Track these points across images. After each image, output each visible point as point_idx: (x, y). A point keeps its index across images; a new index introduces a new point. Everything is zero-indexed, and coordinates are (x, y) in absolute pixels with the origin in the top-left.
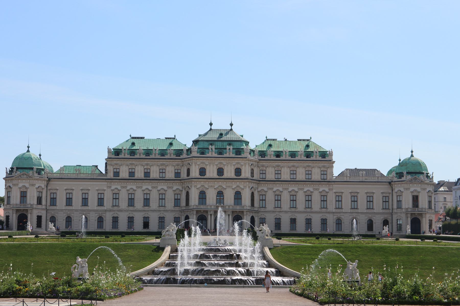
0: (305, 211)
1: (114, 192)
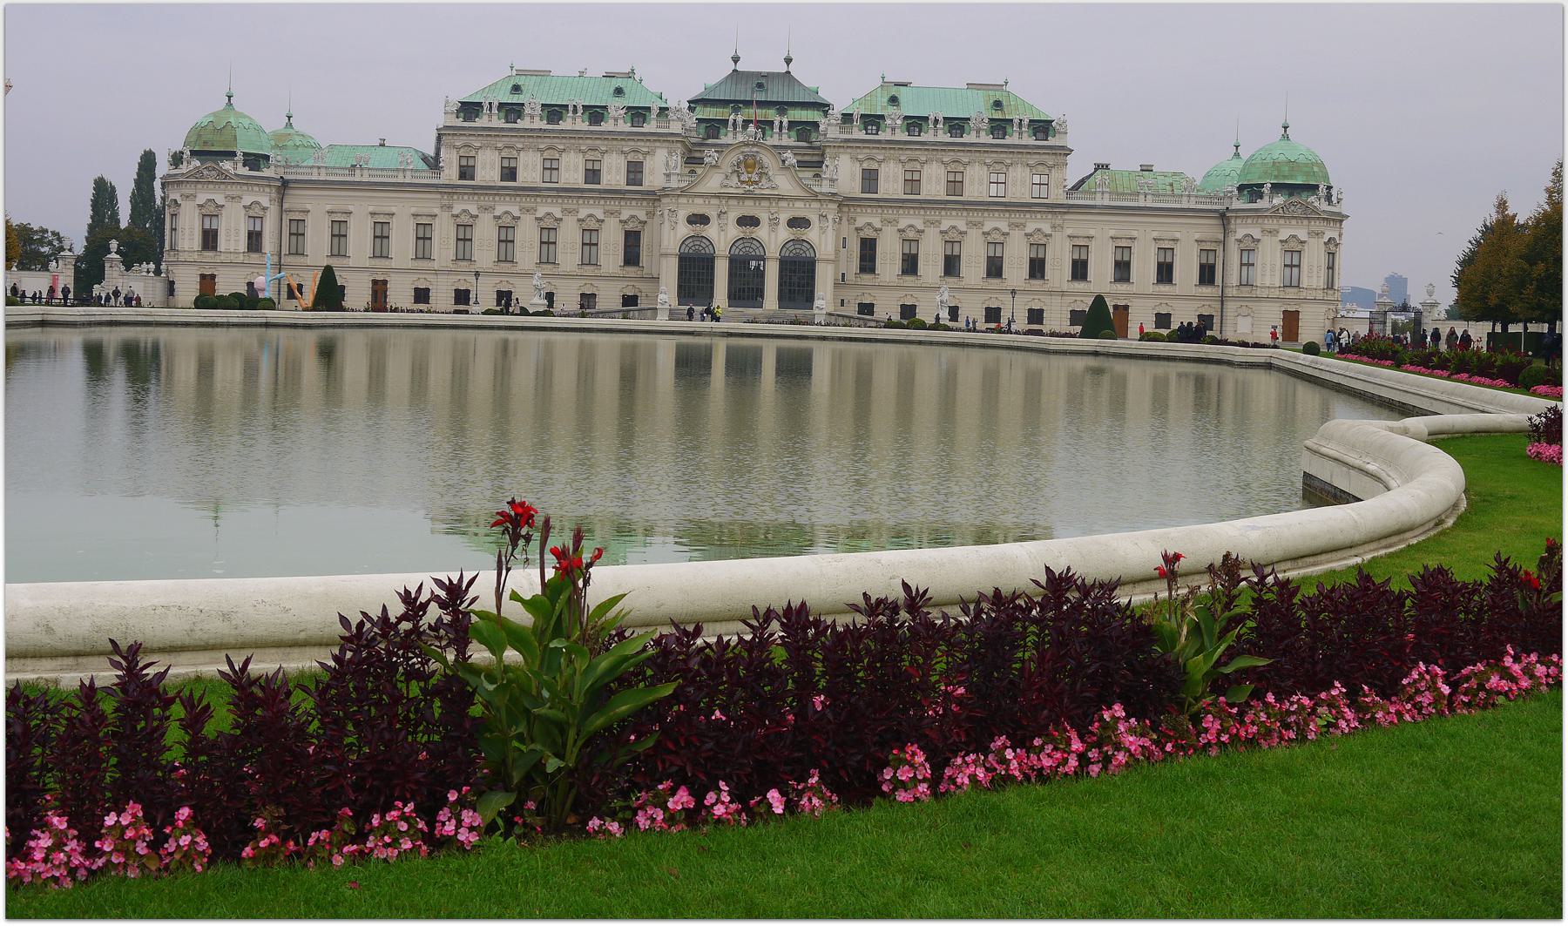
0: (985, 286)
1: (459, 221)
